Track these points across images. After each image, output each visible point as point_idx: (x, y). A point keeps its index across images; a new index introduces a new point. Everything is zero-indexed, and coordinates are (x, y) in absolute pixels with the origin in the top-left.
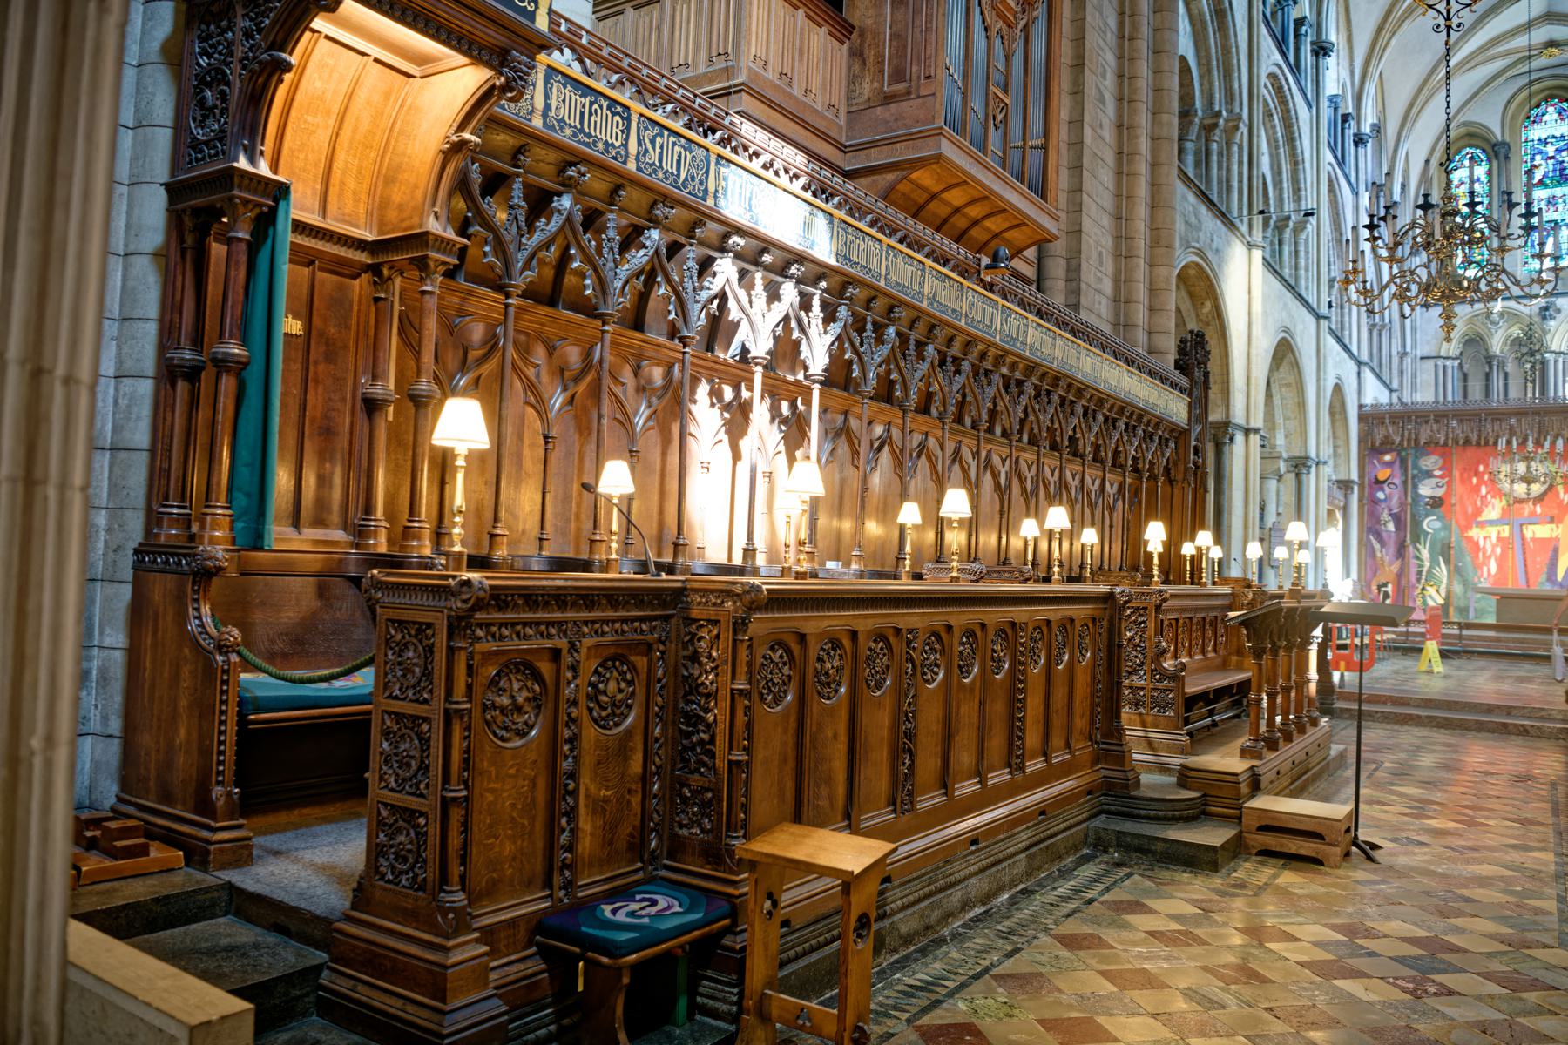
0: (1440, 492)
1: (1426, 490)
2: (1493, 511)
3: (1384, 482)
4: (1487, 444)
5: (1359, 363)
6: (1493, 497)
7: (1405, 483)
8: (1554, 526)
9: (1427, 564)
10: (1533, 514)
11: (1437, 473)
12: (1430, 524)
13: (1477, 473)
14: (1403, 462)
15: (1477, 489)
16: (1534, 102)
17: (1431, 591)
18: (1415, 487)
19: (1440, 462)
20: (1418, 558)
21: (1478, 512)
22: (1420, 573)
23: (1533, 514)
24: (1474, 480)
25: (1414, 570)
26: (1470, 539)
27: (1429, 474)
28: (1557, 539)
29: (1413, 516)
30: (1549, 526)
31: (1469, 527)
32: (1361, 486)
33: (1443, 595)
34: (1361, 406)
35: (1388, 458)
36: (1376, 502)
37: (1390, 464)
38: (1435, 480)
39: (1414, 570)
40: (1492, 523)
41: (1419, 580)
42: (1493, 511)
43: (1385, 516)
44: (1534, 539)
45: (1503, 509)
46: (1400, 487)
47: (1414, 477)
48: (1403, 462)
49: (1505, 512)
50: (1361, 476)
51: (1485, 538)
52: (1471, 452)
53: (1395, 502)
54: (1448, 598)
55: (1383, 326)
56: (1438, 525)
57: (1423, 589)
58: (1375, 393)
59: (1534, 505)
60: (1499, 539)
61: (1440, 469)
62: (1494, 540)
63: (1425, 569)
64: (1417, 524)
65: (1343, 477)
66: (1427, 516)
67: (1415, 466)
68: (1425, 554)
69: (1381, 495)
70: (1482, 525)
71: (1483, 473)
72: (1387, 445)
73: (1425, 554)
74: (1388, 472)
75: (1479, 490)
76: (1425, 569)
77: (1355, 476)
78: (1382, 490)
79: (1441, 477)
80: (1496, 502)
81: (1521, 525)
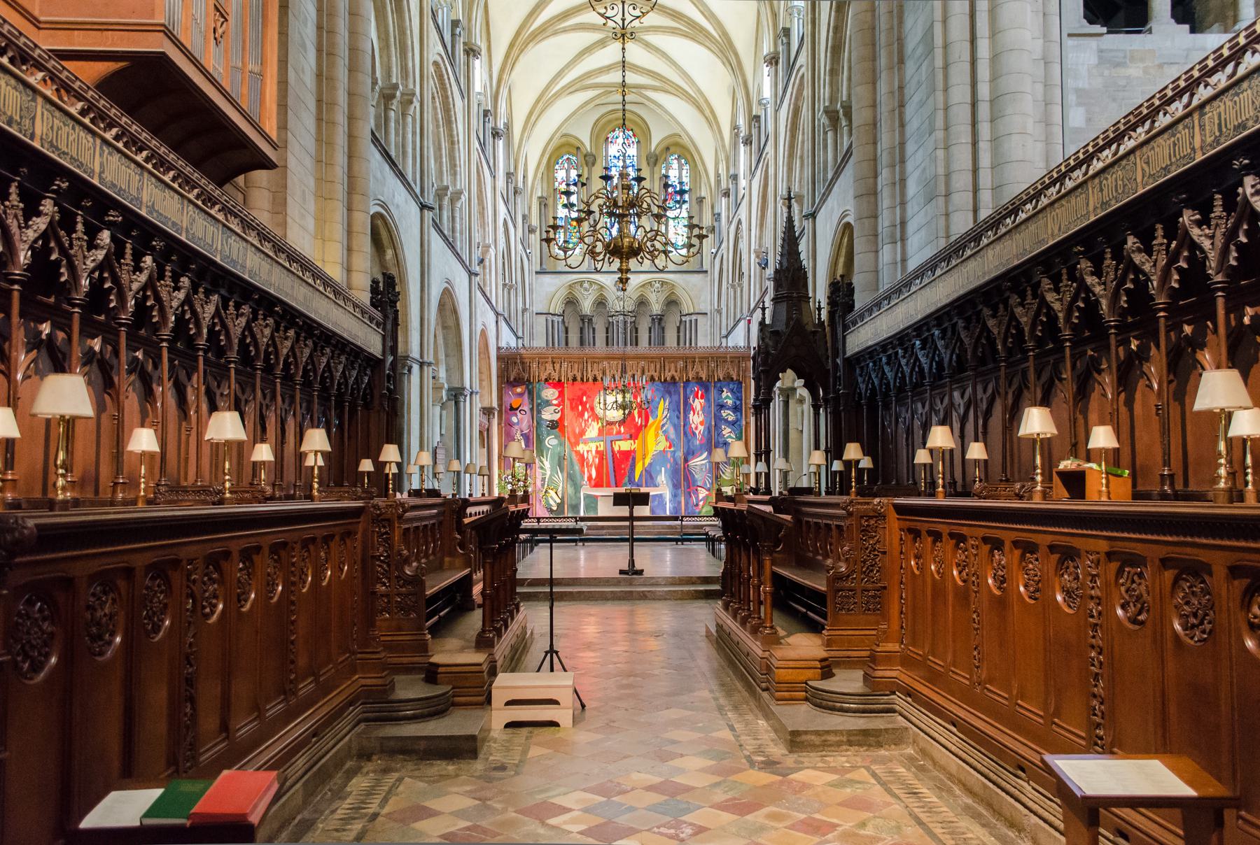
0: (557, 417)
1: (549, 415)
2: (593, 431)
3: (517, 409)
4: (588, 380)
5: (497, 314)
6: (593, 420)
7: (532, 409)
9: (548, 473)
10: (619, 433)
11: (555, 402)
12: (551, 441)
14: (531, 393)
15: (582, 415)
16: (611, 127)
17: (552, 493)
18: (539, 412)
19: (557, 394)
20: (542, 468)
21: (583, 433)
22: (543, 480)
23: (619, 433)
25: (539, 478)
26: (577, 452)
27: (548, 403)
28: (634, 451)
29: (538, 436)
30: (629, 442)
31: (577, 443)
32: (500, 412)
34: (499, 348)
35: (519, 390)
36: (511, 425)
37: (521, 395)
39: (539, 478)
40: (592, 440)
41: (543, 485)
42: (593, 431)
43: (518, 436)
44: (621, 452)
46: (528, 412)
47: (539, 405)
48: (531, 393)
49: (601, 432)
50: (500, 405)
53: (525, 425)
54: (562, 499)
55: (511, 287)
56: (555, 442)
57: (546, 492)
58: (508, 340)
60: (597, 452)
62: (594, 453)
63: (547, 477)
64: (540, 441)
65: (486, 405)
66: (548, 435)
67: (539, 397)
68: (547, 464)
69: (514, 419)
70: (586, 442)
71: (586, 403)
72: (518, 381)
73: (547, 464)
74: (519, 400)
76: (547, 477)
77: (495, 404)
78: (516, 416)
80: (595, 424)
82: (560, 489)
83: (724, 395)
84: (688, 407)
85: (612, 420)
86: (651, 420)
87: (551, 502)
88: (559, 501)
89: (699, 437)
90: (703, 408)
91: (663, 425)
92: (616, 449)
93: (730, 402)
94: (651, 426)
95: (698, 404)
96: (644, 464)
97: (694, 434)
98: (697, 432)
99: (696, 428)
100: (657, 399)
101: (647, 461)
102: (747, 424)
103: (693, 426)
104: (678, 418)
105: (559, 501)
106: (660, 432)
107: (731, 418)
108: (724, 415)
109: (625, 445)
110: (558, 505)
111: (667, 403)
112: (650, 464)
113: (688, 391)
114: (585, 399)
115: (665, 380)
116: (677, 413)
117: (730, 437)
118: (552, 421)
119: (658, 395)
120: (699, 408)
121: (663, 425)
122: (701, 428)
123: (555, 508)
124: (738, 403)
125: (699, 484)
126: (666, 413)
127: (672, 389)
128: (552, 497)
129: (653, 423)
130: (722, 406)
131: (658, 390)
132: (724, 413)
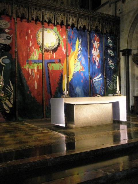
0: (8, 42)
8: (61, 64)
13: (27, 34)
19: (9, 25)
21: (28, 55)
23: (52, 57)
24: (26, 38)
33: (12, 102)
38: (5, 35)
40: (34, 62)
44: (53, 71)
45: (39, 54)
51: (32, 70)
52: (25, 23)
54: (14, 104)
59: (53, 53)
60: (38, 70)
61: (8, 29)
70: (30, 62)
71: (31, 34)
75: (29, 44)
79: (8, 33)
80: (36, 50)
81: (48, 63)
82: (12, 97)
83: (109, 41)
84: (91, 46)
85: (48, 49)
86: (72, 51)
87: (5, 107)
88: (11, 106)
89: (97, 64)
90: (99, 48)
91: (79, 55)
92: (50, 69)
93: (111, 45)
94: (72, 55)
95: (96, 44)
96: (68, 78)
97: (95, 62)
98: (96, 61)
99: (96, 59)
100: (75, 38)
101: (71, 77)
102: (120, 59)
103: (94, 57)
104: (86, 51)
105: (11, 106)
106: (77, 60)
107: (112, 55)
108: (109, 52)
109: (56, 67)
110: (10, 109)
111: (80, 42)
112: (72, 80)
113: (91, 35)
114: (29, 32)
115: (80, 27)
116: (85, 48)
117: (112, 65)
118: (5, 45)
119: (76, 35)
120: (97, 47)
121: (79, 55)
122: (98, 59)
123: (8, 112)
124: (115, 46)
125: (98, 92)
126: (80, 47)
127: (83, 33)
128: (5, 104)
129: (73, 53)
130: (108, 47)
131: (75, 32)
132: (109, 51)
